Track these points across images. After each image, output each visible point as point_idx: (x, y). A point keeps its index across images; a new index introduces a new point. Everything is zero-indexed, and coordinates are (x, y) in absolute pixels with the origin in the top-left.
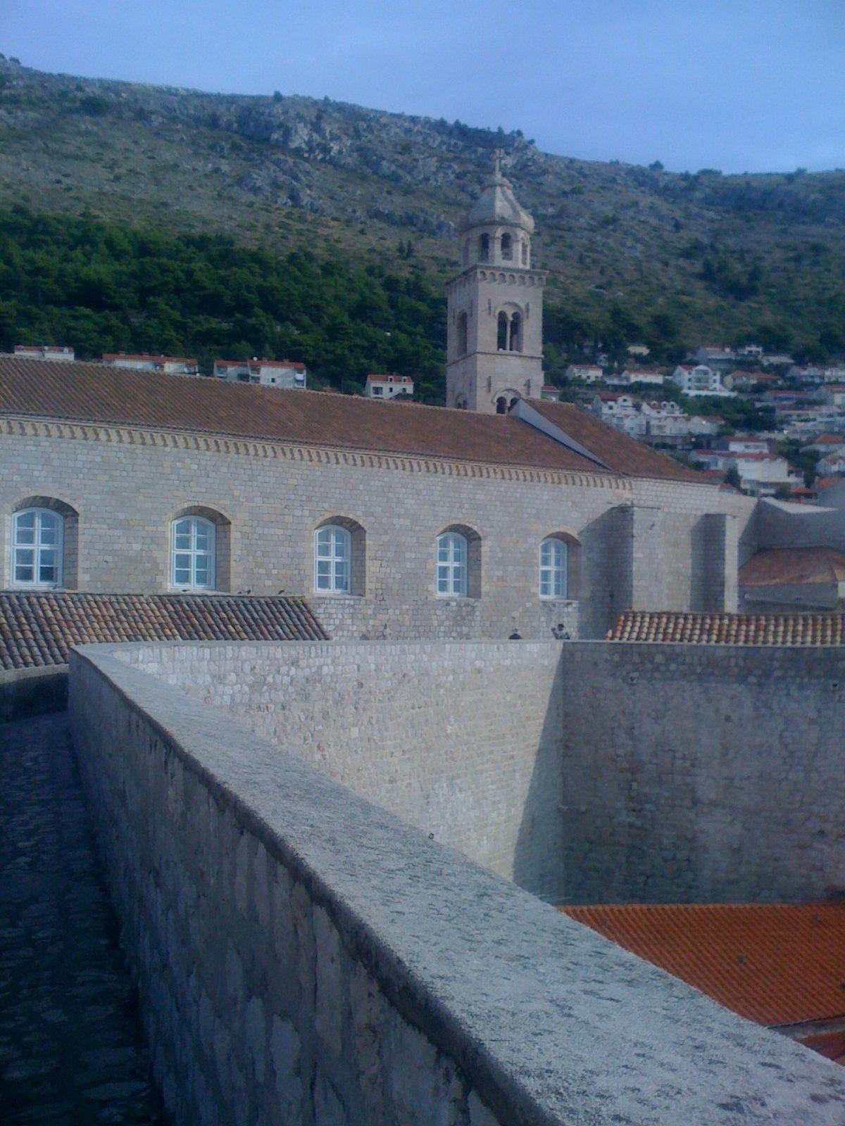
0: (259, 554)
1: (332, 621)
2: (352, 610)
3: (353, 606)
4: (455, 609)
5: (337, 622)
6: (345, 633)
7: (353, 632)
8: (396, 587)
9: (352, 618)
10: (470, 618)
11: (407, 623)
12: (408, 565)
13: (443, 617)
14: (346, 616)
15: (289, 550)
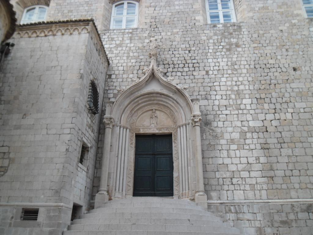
0: (66, 11)
1: (114, 42)
2: (130, 35)
3: (131, 33)
4: (224, 28)
5: (118, 42)
6: (124, 48)
7: (130, 47)
8: (167, 20)
9: (131, 39)
10: (237, 33)
11: (178, 38)
12: (177, 7)
13: (212, 34)
14: (125, 39)
15: (87, 8)
